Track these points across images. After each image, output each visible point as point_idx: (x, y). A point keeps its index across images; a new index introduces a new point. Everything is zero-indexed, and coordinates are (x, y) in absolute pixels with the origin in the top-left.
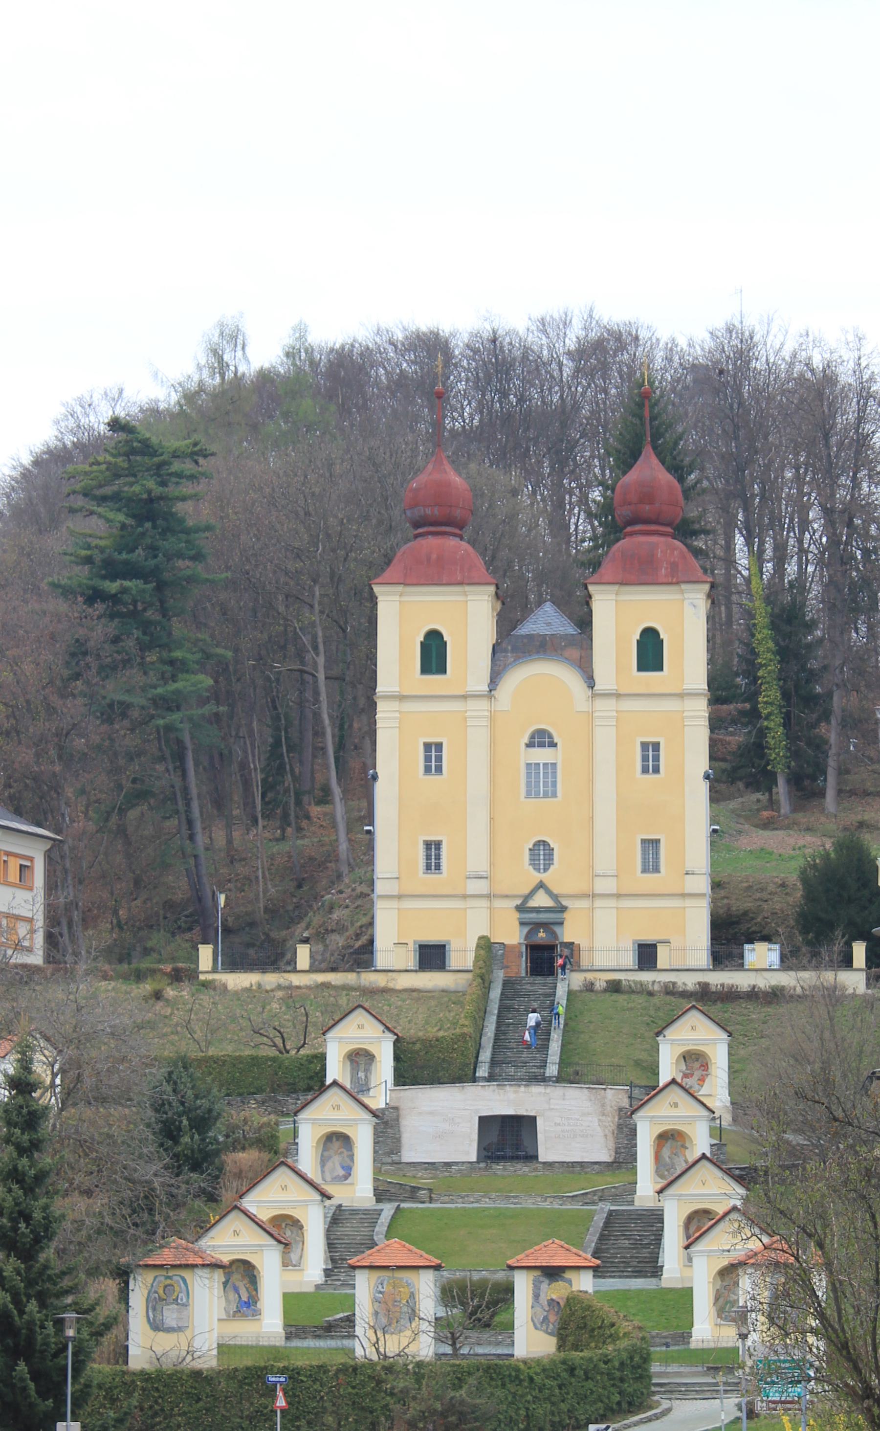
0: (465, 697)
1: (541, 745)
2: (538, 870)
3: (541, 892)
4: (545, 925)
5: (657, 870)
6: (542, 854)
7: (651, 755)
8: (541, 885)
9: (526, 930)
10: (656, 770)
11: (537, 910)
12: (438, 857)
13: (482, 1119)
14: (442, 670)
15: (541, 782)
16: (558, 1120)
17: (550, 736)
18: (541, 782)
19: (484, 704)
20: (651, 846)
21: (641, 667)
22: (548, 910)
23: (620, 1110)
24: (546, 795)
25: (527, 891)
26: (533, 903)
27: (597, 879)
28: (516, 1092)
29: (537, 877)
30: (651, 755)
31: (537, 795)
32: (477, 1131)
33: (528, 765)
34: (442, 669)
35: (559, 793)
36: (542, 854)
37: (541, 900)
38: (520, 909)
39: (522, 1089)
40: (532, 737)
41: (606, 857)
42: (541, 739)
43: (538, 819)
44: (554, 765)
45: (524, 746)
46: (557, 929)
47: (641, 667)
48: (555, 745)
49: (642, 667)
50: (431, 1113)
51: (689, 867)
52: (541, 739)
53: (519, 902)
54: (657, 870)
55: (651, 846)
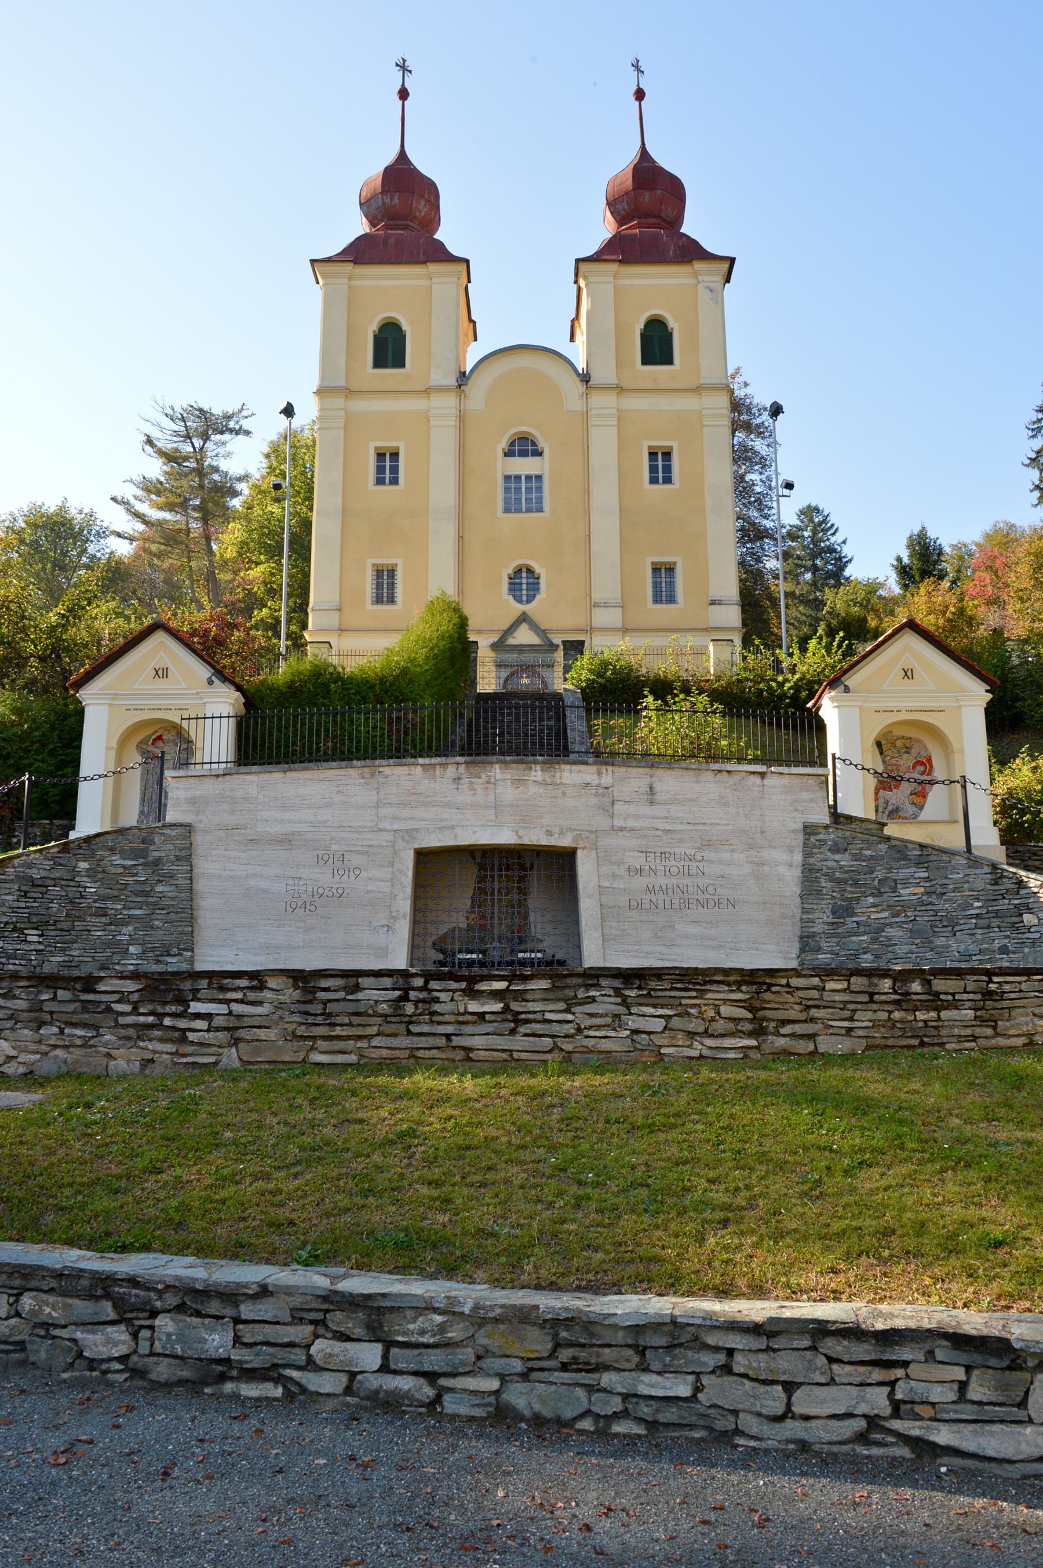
0: (427, 392)
1: (523, 453)
2: (521, 602)
3: (524, 628)
4: (529, 669)
5: (671, 599)
6: (524, 582)
7: (661, 464)
8: (523, 618)
9: (504, 674)
10: (668, 480)
11: (520, 649)
12: (392, 586)
13: (423, 857)
14: (399, 362)
15: (522, 495)
16: (636, 860)
17: (534, 444)
18: (522, 495)
19: (449, 402)
20: (664, 572)
21: (646, 360)
22: (532, 648)
23: (809, 830)
24: (529, 510)
25: (505, 627)
26: (511, 641)
27: (595, 610)
28: (518, 783)
29: (520, 608)
30: (661, 464)
31: (518, 510)
32: (409, 890)
33: (507, 478)
34: (399, 362)
35: (546, 506)
36: (524, 582)
37: (524, 636)
38: (494, 647)
39: (537, 773)
40: (512, 444)
41: (606, 583)
42: (523, 446)
43: (518, 537)
44: (539, 478)
45: (500, 454)
46: (545, 673)
47: (646, 360)
48: (541, 454)
49: (647, 359)
50: (286, 841)
51: (715, 593)
52: (523, 446)
53: (495, 638)
54: (671, 599)
55: (664, 572)
